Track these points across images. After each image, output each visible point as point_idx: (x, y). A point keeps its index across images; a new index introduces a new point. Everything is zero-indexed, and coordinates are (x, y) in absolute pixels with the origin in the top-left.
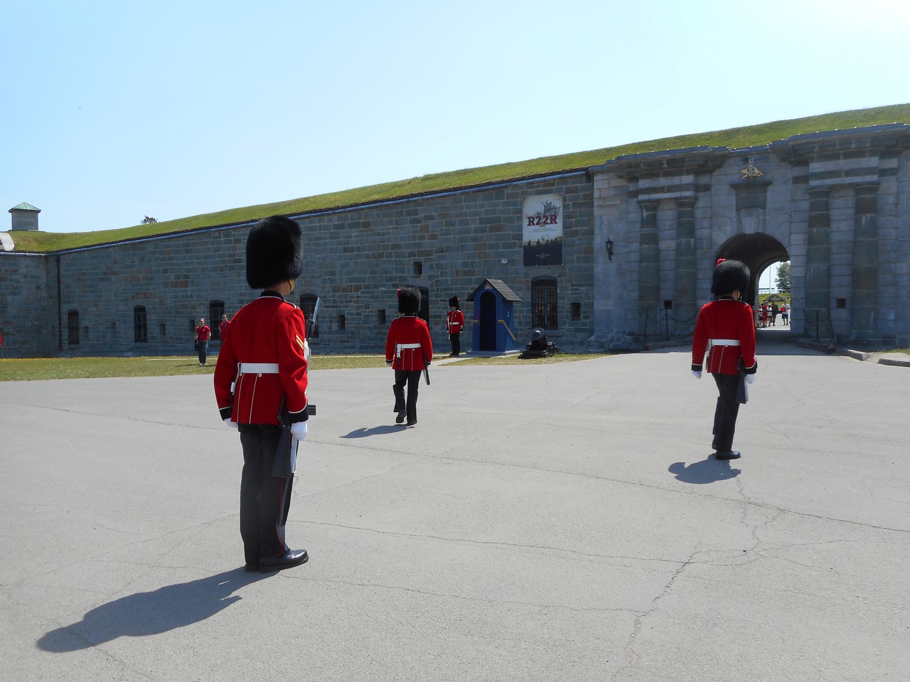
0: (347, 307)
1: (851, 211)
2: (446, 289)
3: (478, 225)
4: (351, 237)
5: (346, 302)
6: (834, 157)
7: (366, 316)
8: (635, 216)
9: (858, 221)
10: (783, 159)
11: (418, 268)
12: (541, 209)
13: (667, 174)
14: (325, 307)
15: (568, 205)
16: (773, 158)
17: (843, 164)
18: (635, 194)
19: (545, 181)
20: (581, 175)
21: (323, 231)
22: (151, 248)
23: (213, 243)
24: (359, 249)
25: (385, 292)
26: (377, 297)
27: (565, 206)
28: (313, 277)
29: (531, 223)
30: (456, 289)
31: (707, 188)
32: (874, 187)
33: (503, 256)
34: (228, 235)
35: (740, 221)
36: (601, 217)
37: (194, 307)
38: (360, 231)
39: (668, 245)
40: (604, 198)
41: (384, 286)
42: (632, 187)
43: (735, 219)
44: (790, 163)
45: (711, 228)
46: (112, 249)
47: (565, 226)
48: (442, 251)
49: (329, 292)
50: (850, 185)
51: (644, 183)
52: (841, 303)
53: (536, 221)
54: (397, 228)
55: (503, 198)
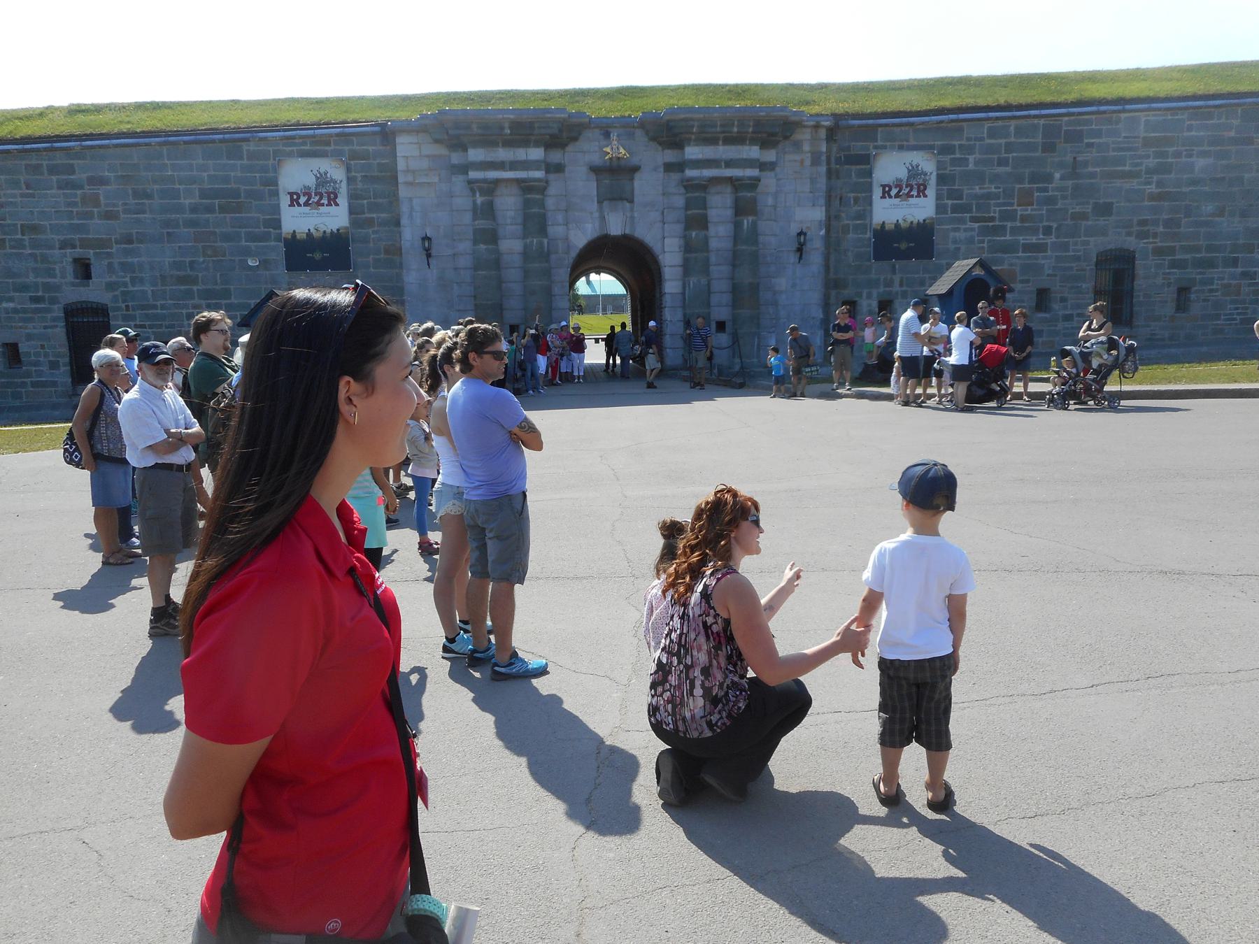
1: (729, 213)
2: (143, 307)
3: (197, 200)
6: (712, 141)
8: (463, 201)
9: (737, 226)
10: (653, 139)
11: (84, 270)
12: (310, 181)
13: (509, 144)
15: (355, 177)
16: (639, 133)
17: (722, 151)
18: (464, 169)
19: (314, 136)
20: (374, 133)
25: (15, 311)
27: (350, 180)
29: (294, 201)
30: (163, 307)
31: (559, 168)
32: (753, 184)
33: (247, 252)
35: (603, 218)
36: (410, 199)
39: (511, 246)
40: (414, 172)
41: (11, 300)
42: (456, 158)
43: (596, 215)
44: (660, 144)
45: (567, 224)
47: (352, 211)
48: (129, 241)
50: (730, 180)
51: (476, 155)
52: (721, 326)
53: (303, 200)
54: (32, 196)
55: (241, 158)
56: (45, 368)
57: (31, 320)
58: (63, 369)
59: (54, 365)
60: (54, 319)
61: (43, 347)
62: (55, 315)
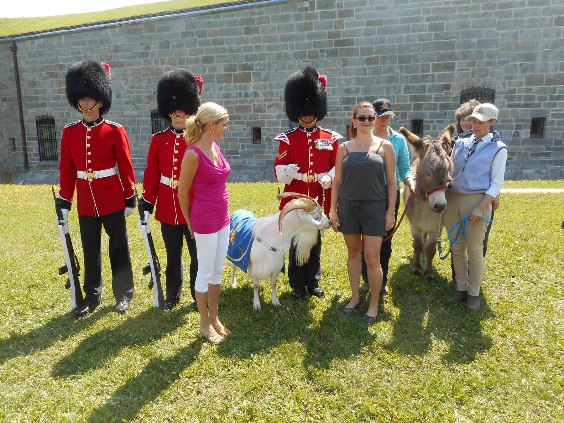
0: (554, 105)
5: (552, 98)
14: (509, 106)
23: (298, 18)
28: (490, 64)
37: (259, 110)
46: (109, 31)
49: (520, 84)
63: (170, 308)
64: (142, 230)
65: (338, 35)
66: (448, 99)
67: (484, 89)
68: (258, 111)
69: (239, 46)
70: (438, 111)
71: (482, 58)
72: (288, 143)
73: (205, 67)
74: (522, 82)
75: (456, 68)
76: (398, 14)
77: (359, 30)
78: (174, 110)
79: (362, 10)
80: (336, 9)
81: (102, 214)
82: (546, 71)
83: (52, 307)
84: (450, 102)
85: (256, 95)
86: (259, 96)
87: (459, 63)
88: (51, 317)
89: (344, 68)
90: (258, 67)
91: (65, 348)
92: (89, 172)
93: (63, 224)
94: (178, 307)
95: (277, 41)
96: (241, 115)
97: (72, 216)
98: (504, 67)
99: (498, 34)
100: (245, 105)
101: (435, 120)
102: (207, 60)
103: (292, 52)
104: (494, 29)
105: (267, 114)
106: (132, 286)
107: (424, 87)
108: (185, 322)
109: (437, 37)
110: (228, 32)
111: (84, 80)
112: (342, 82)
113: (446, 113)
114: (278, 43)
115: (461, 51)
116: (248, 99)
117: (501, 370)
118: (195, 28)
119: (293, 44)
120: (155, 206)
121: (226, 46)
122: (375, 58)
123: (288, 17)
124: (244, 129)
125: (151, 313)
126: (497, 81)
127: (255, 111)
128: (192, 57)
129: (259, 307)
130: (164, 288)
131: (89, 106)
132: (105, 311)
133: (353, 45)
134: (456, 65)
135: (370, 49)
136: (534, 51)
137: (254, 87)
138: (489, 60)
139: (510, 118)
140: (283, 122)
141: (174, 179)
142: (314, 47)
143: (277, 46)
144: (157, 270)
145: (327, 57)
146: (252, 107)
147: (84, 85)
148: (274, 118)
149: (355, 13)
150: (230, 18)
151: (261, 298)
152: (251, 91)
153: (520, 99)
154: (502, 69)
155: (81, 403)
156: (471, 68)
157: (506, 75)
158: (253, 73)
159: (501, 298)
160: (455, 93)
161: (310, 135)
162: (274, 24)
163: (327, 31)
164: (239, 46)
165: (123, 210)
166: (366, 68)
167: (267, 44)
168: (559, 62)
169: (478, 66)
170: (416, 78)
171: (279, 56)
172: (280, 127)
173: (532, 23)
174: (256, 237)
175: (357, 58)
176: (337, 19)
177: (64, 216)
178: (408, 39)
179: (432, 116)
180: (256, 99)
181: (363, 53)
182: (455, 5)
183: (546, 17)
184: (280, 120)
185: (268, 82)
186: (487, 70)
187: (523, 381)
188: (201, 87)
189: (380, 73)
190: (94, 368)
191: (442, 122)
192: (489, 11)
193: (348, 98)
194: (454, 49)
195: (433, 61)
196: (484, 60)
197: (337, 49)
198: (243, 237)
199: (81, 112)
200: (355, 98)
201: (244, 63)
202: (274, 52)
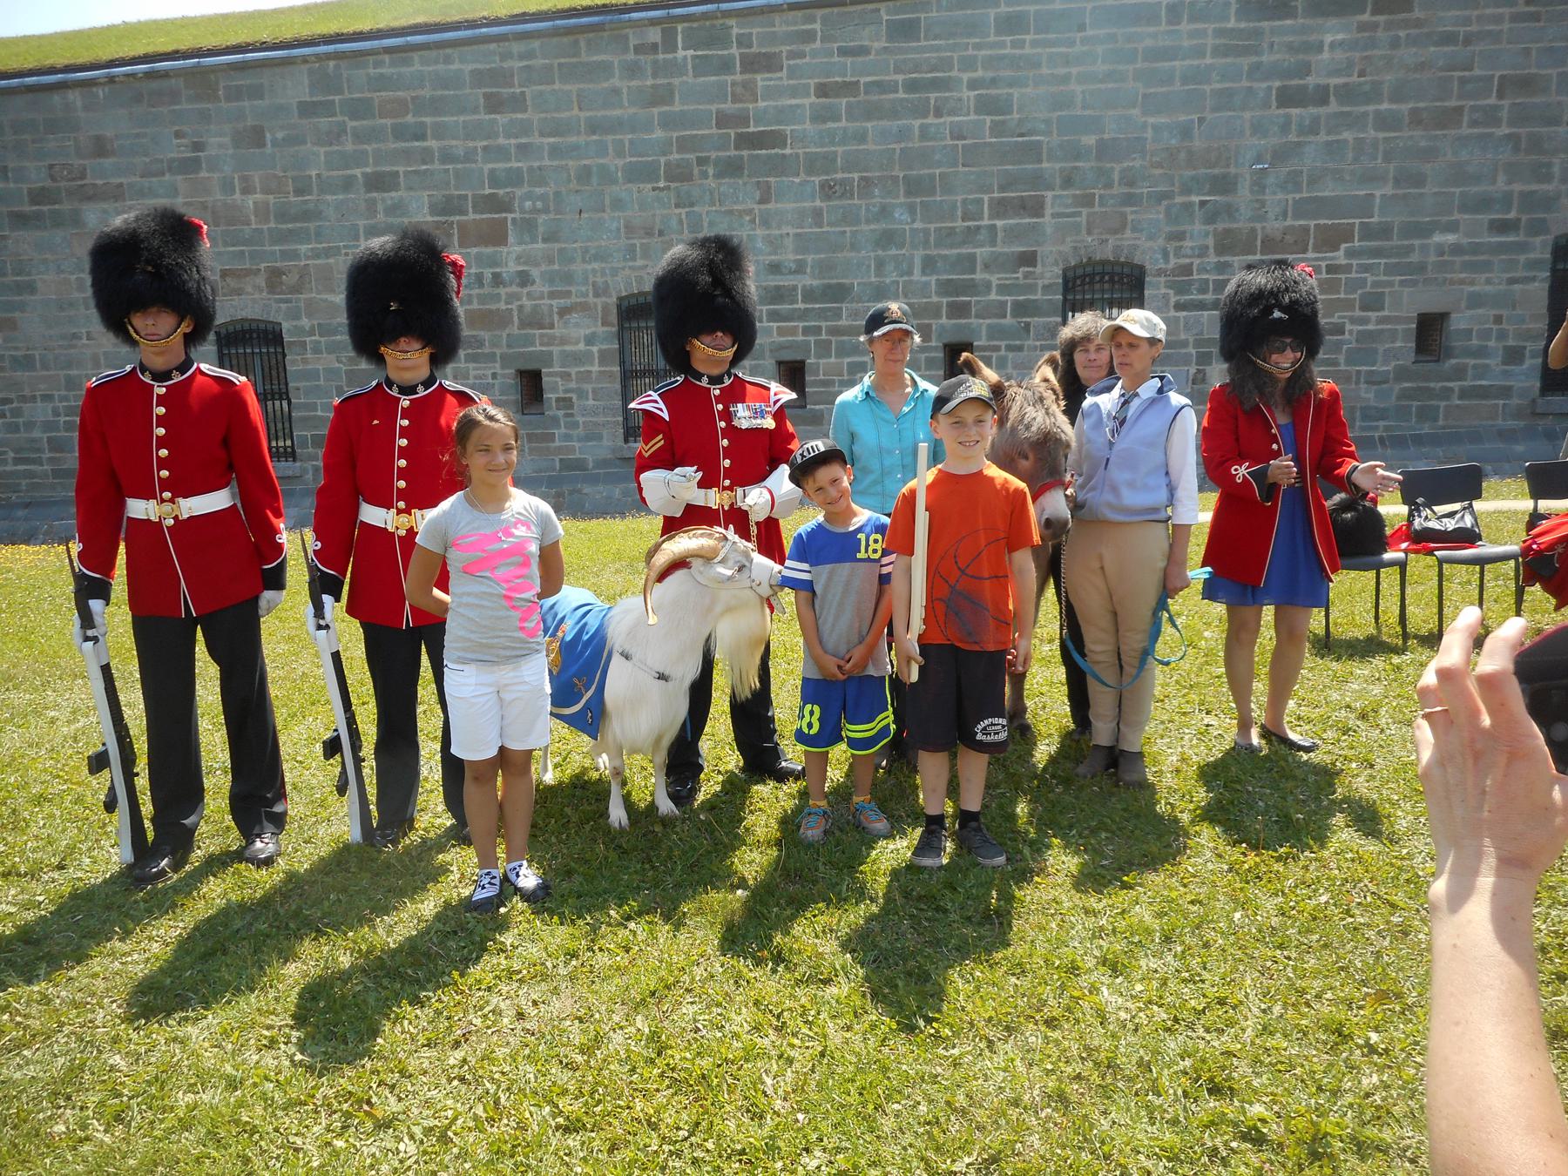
4: (1319, 47)
7: (1363, 336)
21: (1185, 26)
22: (296, 89)
23: (632, 70)
24: (1348, 94)
25: (1457, 249)
26: (1422, 268)
28: (1129, 200)
34: (720, 39)
37: (534, 320)
38: (1362, 27)
41: (1452, 227)
46: (74, 96)
49: (1203, 251)
54: (1536, 17)
56: (1494, 362)
57: (1486, 267)
58: (1528, 363)
59: (1514, 356)
60: (1533, 265)
61: (1498, 319)
62: (1532, 256)
63: (395, 842)
64: (308, 646)
65: (744, 120)
66: (1031, 289)
67: (1117, 263)
68: (530, 325)
69: (471, 144)
70: (1008, 320)
71: (1109, 185)
72: (666, 416)
73: (373, 202)
74: (1207, 247)
75: (1048, 211)
76: (898, 70)
77: (798, 106)
78: (392, 337)
79: (802, 55)
80: (735, 51)
81: (196, 607)
82: (1262, 218)
83: (61, 867)
84: (1038, 297)
85: (524, 279)
86: (533, 282)
87: (1055, 197)
88: (66, 890)
89: (763, 207)
90: (528, 204)
91: (148, 948)
92: (163, 501)
93: (95, 639)
94: (414, 838)
95: (579, 133)
96: (485, 335)
97: (116, 616)
98: (1162, 208)
99: (1145, 125)
100: (493, 307)
101: (1003, 344)
102: (378, 182)
103: (620, 162)
104: (1135, 112)
105: (557, 332)
106: (281, 795)
107: (972, 259)
108: (444, 870)
109: (998, 129)
110: (436, 106)
111: (148, 262)
112: (760, 245)
113: (1028, 325)
114: (581, 140)
115: (1058, 166)
116: (502, 291)
117: (1192, 902)
118: (340, 91)
119: (621, 141)
120: (347, 580)
121: (432, 143)
122: (843, 182)
123: (606, 68)
124: (494, 376)
125: (343, 856)
126: (1149, 244)
127: (523, 325)
128: (335, 173)
129: (625, 821)
130: (372, 791)
131: (158, 331)
132: (217, 863)
133: (784, 146)
134: (1048, 201)
135: (829, 159)
136: (1233, 170)
137: (518, 258)
138: (1126, 190)
139: (1183, 337)
140: (602, 353)
141: (399, 512)
142: (681, 149)
143: (576, 147)
144: (356, 745)
145: (716, 176)
146: (515, 313)
147: (143, 273)
148: (577, 343)
149: (785, 63)
150: (441, 67)
151: (627, 799)
152: (512, 267)
153: (1203, 290)
154: (1157, 214)
155: (229, 1069)
156: (1085, 211)
157: (1168, 229)
158: (514, 220)
159: (1183, 760)
160: (1048, 275)
161: (717, 392)
162: (568, 87)
163: (714, 108)
164: (471, 144)
165: (256, 599)
166: (821, 209)
167: (552, 140)
168: (1290, 197)
169: (1101, 205)
170: (949, 235)
171: (585, 175)
172: (595, 368)
173: (1224, 100)
174: (617, 648)
175: (797, 180)
176: (738, 77)
177: (97, 620)
178: (924, 133)
179: (995, 332)
180: (525, 291)
181: (811, 171)
182: (1039, 50)
183: (1256, 85)
184: (595, 349)
185: (557, 246)
186: (1124, 216)
187: (1237, 915)
188: (459, 278)
189: (857, 222)
190: (238, 991)
191: (1020, 349)
192: (1121, 67)
193: (778, 288)
194: (1040, 161)
195: (990, 190)
196: (1115, 191)
197: (742, 157)
198: (582, 653)
199: (134, 343)
200: (795, 288)
201: (487, 191)
202: (571, 163)
